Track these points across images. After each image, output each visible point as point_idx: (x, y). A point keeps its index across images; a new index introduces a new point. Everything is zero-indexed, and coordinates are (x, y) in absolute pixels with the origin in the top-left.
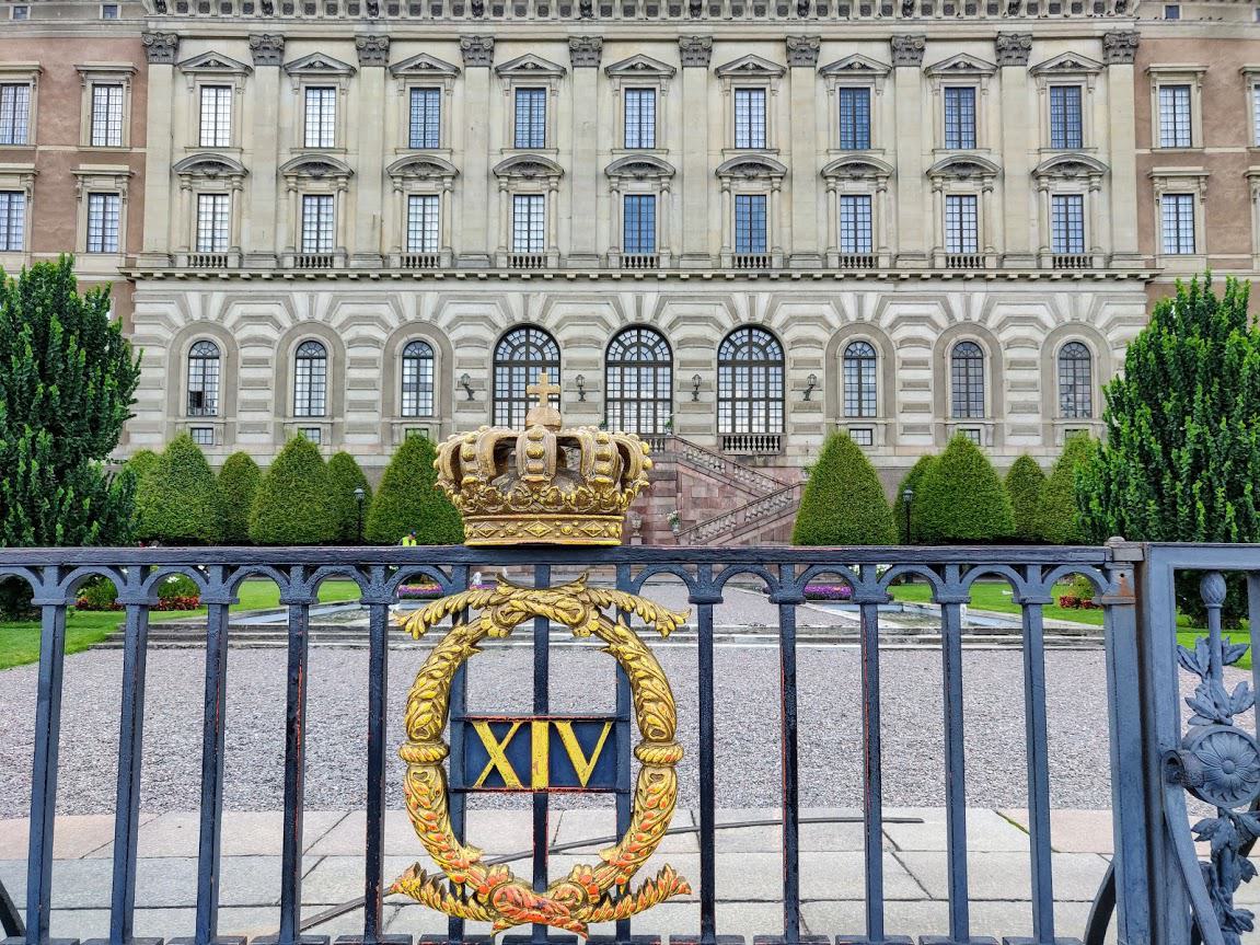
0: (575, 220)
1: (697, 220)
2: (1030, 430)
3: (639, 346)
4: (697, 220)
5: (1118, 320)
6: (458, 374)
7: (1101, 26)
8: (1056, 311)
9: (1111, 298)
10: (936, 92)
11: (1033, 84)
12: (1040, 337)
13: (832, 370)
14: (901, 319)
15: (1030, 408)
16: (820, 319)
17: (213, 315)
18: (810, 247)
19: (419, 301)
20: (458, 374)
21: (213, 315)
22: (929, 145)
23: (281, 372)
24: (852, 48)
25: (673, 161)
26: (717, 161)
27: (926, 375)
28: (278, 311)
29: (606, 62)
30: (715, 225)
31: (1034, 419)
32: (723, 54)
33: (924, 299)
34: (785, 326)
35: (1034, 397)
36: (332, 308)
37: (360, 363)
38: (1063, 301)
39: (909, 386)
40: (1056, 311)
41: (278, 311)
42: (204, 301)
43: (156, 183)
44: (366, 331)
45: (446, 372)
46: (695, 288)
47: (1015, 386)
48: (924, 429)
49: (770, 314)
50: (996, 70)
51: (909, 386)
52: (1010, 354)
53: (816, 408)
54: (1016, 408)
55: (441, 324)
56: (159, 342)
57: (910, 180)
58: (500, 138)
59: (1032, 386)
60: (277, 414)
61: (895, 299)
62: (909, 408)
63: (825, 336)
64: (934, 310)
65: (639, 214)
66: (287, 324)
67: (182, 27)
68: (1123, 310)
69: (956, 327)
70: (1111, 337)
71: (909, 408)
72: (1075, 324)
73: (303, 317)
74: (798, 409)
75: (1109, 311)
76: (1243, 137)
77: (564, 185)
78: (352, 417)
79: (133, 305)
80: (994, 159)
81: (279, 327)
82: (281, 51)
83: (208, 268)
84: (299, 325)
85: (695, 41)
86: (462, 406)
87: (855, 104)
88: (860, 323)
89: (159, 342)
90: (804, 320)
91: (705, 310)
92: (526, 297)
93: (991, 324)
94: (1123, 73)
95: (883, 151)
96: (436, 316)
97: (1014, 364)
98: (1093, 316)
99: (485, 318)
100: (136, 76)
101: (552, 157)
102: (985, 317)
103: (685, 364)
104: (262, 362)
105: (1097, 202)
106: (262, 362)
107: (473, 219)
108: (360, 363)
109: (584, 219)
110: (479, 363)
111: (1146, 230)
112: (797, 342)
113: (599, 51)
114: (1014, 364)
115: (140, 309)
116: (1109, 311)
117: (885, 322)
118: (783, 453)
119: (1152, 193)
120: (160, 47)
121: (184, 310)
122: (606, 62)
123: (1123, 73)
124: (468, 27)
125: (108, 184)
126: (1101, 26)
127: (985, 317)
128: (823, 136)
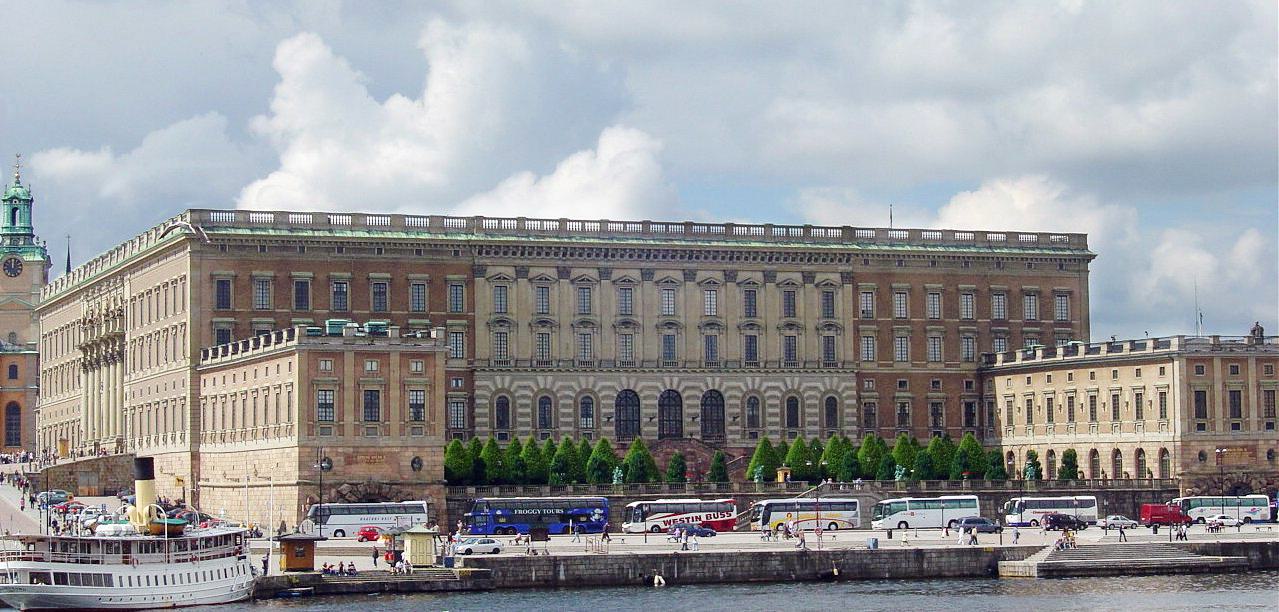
0: (646, 346)
1: (691, 346)
2: (815, 432)
3: (671, 401)
4: (691, 346)
5: (847, 388)
6: (604, 411)
7: (842, 268)
8: (824, 384)
9: (844, 380)
10: (781, 293)
11: (816, 290)
12: (819, 395)
13: (743, 408)
14: (768, 388)
15: (815, 424)
16: (738, 388)
17: (506, 385)
18: (734, 358)
19: (586, 381)
20: (604, 411)
21: (506, 385)
22: (778, 315)
23: (533, 409)
24: (749, 275)
25: (682, 320)
26: (697, 321)
27: (778, 410)
28: (531, 384)
29: (656, 278)
30: (698, 348)
31: (817, 428)
32: (701, 275)
33: (776, 380)
34: (726, 390)
35: (817, 419)
36: (553, 383)
37: (564, 406)
38: (827, 380)
39: (771, 415)
40: (824, 384)
41: (531, 384)
42: (503, 381)
43: (481, 330)
44: (567, 393)
45: (598, 410)
46: (693, 375)
47: (810, 415)
48: (776, 432)
49: (720, 385)
50: (803, 285)
51: (771, 415)
52: (808, 402)
53: (737, 424)
54: (810, 424)
55: (596, 390)
56: (485, 397)
57: (772, 331)
58: (614, 310)
59: (815, 414)
60: (533, 427)
61: (766, 380)
62: (771, 424)
63: (740, 395)
64: (780, 384)
65: (669, 341)
66: (536, 390)
67: (488, 262)
68: (848, 384)
69: (789, 391)
70: (844, 395)
71: (771, 424)
72: (831, 390)
73: (542, 387)
74: (731, 424)
75: (843, 384)
76: (890, 315)
77: (641, 331)
78: (563, 429)
79: (473, 382)
80: (802, 322)
81: (533, 391)
82: (528, 272)
83: (503, 365)
84: (540, 390)
85: (690, 270)
86: (606, 424)
87: (751, 296)
88: (753, 390)
89: (485, 397)
90: (733, 388)
91: (696, 384)
92: (628, 378)
93: (801, 390)
94: (849, 287)
95: (761, 318)
96: (594, 386)
97: (810, 406)
98: (838, 387)
99: (613, 388)
100: (470, 283)
101: (635, 319)
102: (799, 388)
103: (689, 406)
104: (526, 406)
105: (838, 340)
106: (526, 406)
107: (607, 345)
108: (564, 406)
109: (648, 346)
110: (610, 406)
111: (857, 352)
112: (731, 397)
113: (653, 274)
114: (810, 406)
115: (477, 383)
116: (843, 384)
117: (763, 389)
118: (725, 442)
119: (859, 336)
120: (478, 271)
121: (495, 383)
122: (656, 278)
123: (849, 287)
124: (602, 264)
125: (460, 329)
126: (842, 268)
127: (799, 388)
128: (738, 310)
